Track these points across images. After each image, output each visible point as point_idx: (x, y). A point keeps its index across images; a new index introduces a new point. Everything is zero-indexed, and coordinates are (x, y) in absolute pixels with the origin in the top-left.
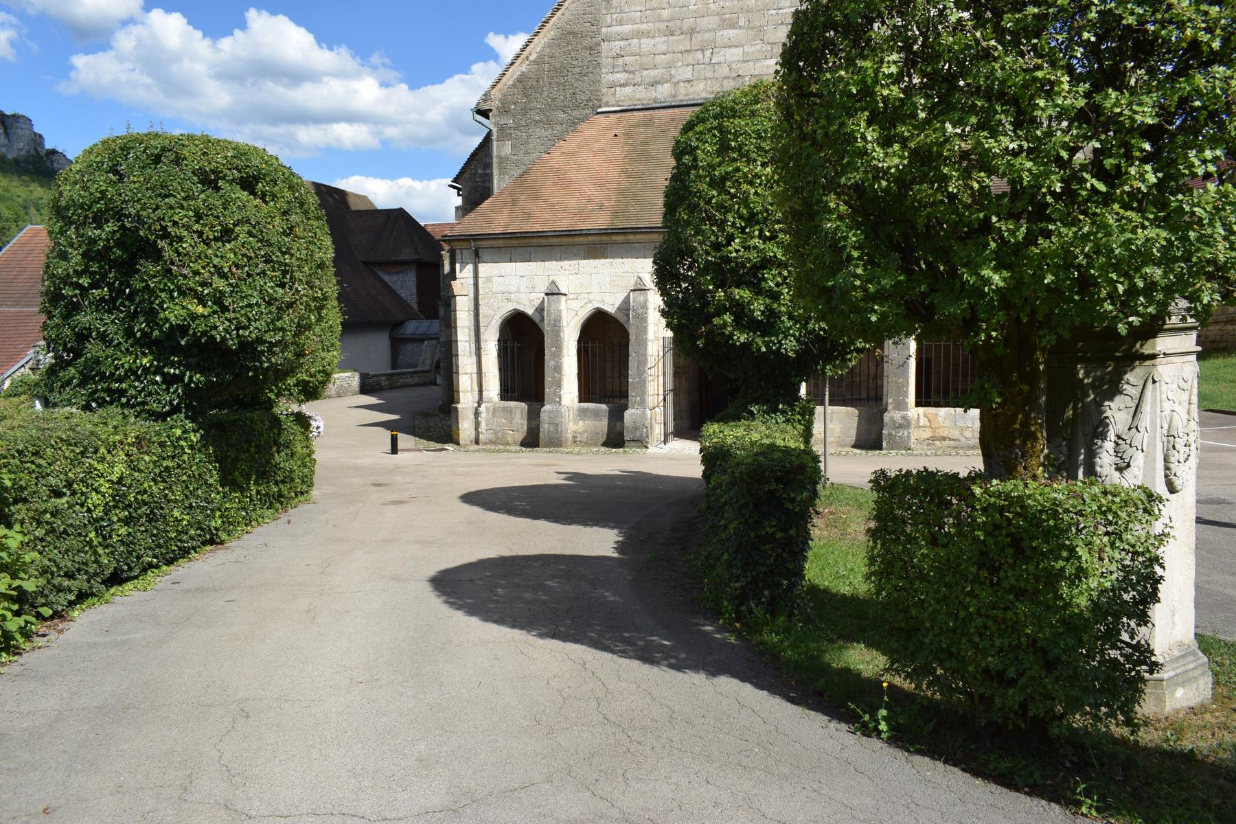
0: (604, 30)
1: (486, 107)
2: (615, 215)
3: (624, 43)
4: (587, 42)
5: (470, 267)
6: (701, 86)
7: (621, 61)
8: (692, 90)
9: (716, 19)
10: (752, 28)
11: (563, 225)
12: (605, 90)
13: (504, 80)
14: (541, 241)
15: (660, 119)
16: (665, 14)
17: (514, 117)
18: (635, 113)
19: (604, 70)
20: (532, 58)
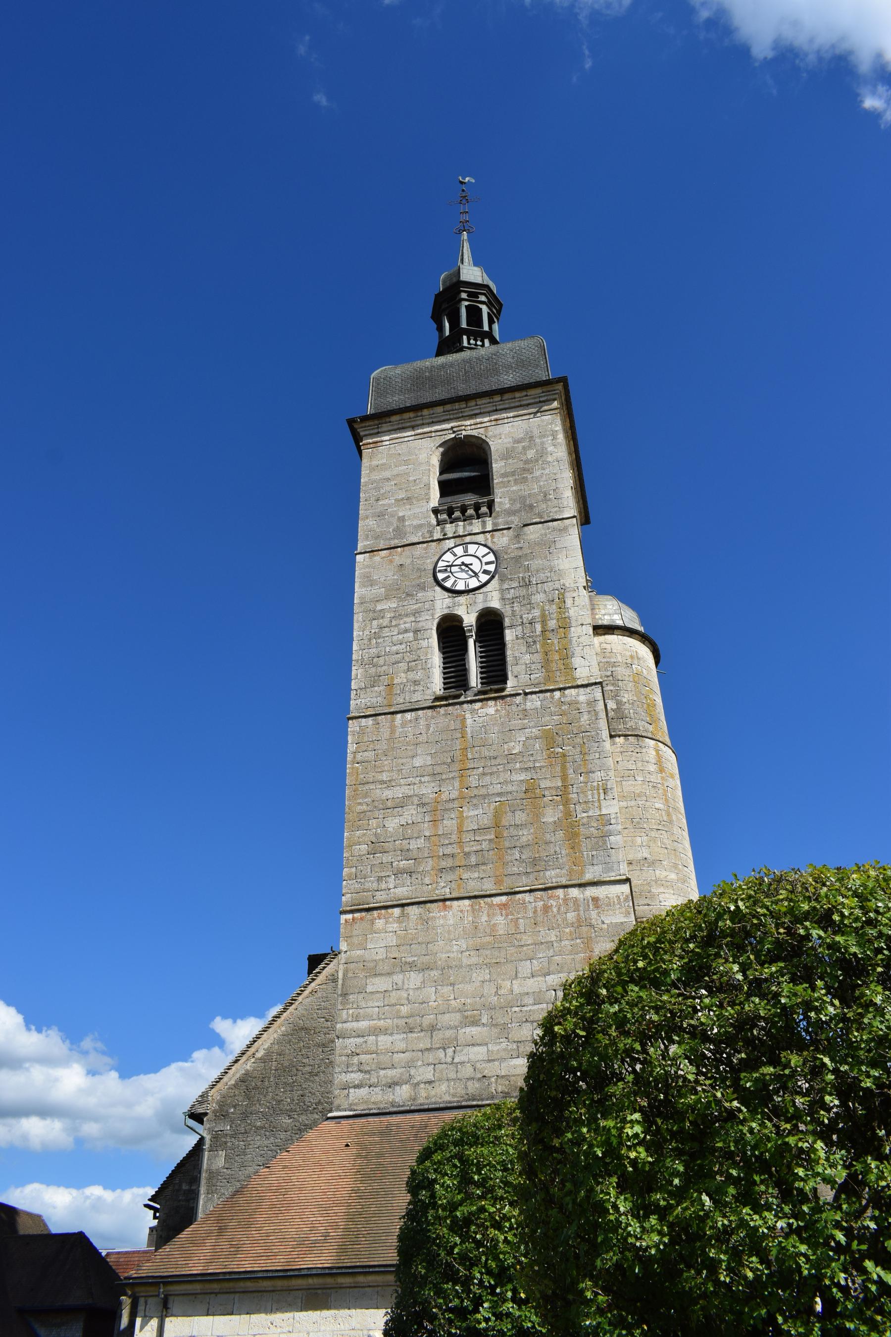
0: (339, 1026)
1: (201, 1111)
2: (342, 1250)
3: (359, 1040)
4: (320, 1038)
5: (154, 1323)
6: (444, 1087)
7: (355, 1060)
8: (433, 1093)
9: (458, 1016)
10: (496, 1025)
11: (277, 1263)
12: (337, 1092)
13: (225, 1079)
14: (249, 1285)
15: (398, 1126)
16: (404, 1010)
17: (232, 1122)
18: (371, 1119)
19: (337, 1070)
20: (259, 1055)
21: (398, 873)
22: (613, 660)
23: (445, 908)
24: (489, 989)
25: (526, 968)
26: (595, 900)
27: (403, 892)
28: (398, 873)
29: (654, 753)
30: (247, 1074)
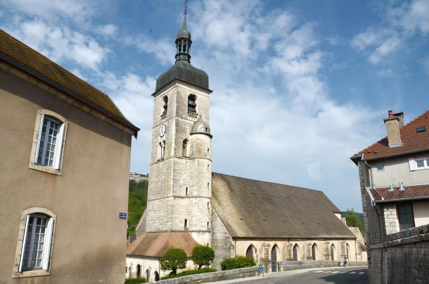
25: (162, 211)
29: (197, 162)
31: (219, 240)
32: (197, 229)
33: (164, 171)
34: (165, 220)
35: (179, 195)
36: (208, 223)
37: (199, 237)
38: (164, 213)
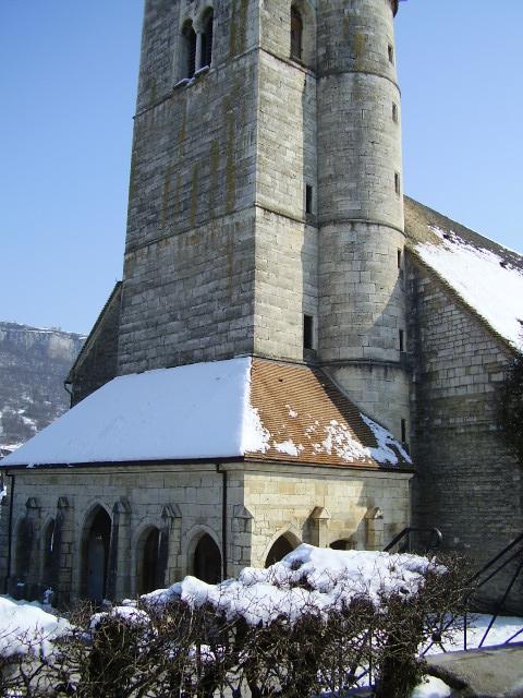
16: (146, 314)
21: (149, 223)
22: (327, 11)
23: (167, 243)
24: (182, 297)
25: (200, 278)
26: (237, 224)
27: (149, 236)
28: (149, 223)
29: (352, 84)
30: (87, 358)
31: (462, 399)
32: (360, 356)
33: (209, 116)
34: (220, 312)
35: (282, 206)
36: (401, 332)
37: (370, 389)
38: (212, 285)
